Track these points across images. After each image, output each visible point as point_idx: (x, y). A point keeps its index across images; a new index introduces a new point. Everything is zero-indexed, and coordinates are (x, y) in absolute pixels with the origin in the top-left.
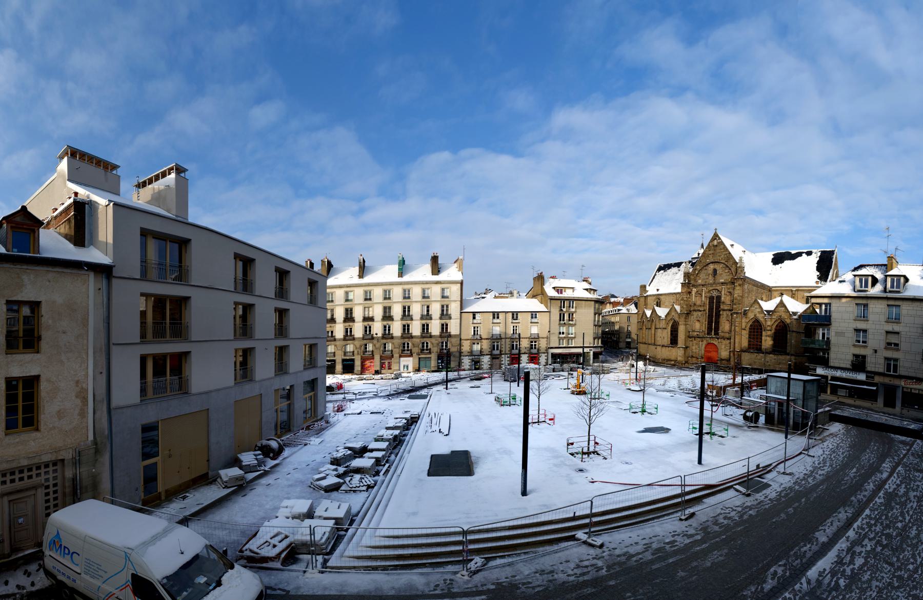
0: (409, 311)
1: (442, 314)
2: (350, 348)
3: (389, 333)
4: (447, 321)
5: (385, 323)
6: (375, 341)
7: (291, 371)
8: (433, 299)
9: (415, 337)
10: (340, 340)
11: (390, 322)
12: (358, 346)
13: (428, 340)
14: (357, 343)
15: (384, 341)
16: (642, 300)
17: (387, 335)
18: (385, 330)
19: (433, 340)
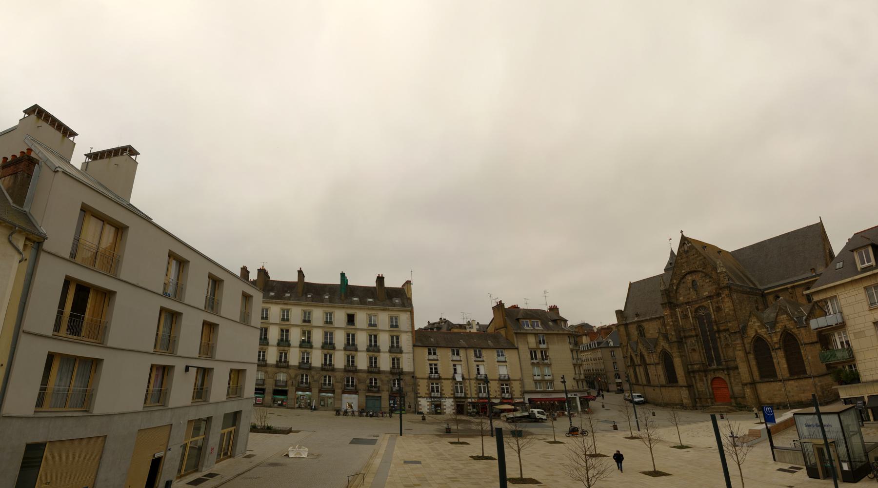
0: (353, 340)
1: (392, 346)
2: (282, 377)
3: (330, 364)
4: (399, 355)
5: (326, 351)
6: (313, 373)
7: (212, 400)
8: (380, 327)
9: (361, 371)
10: (272, 366)
11: (331, 352)
12: (293, 375)
13: (376, 376)
14: (292, 372)
15: (325, 373)
16: (622, 329)
17: (328, 366)
18: (326, 360)
19: (383, 377)
